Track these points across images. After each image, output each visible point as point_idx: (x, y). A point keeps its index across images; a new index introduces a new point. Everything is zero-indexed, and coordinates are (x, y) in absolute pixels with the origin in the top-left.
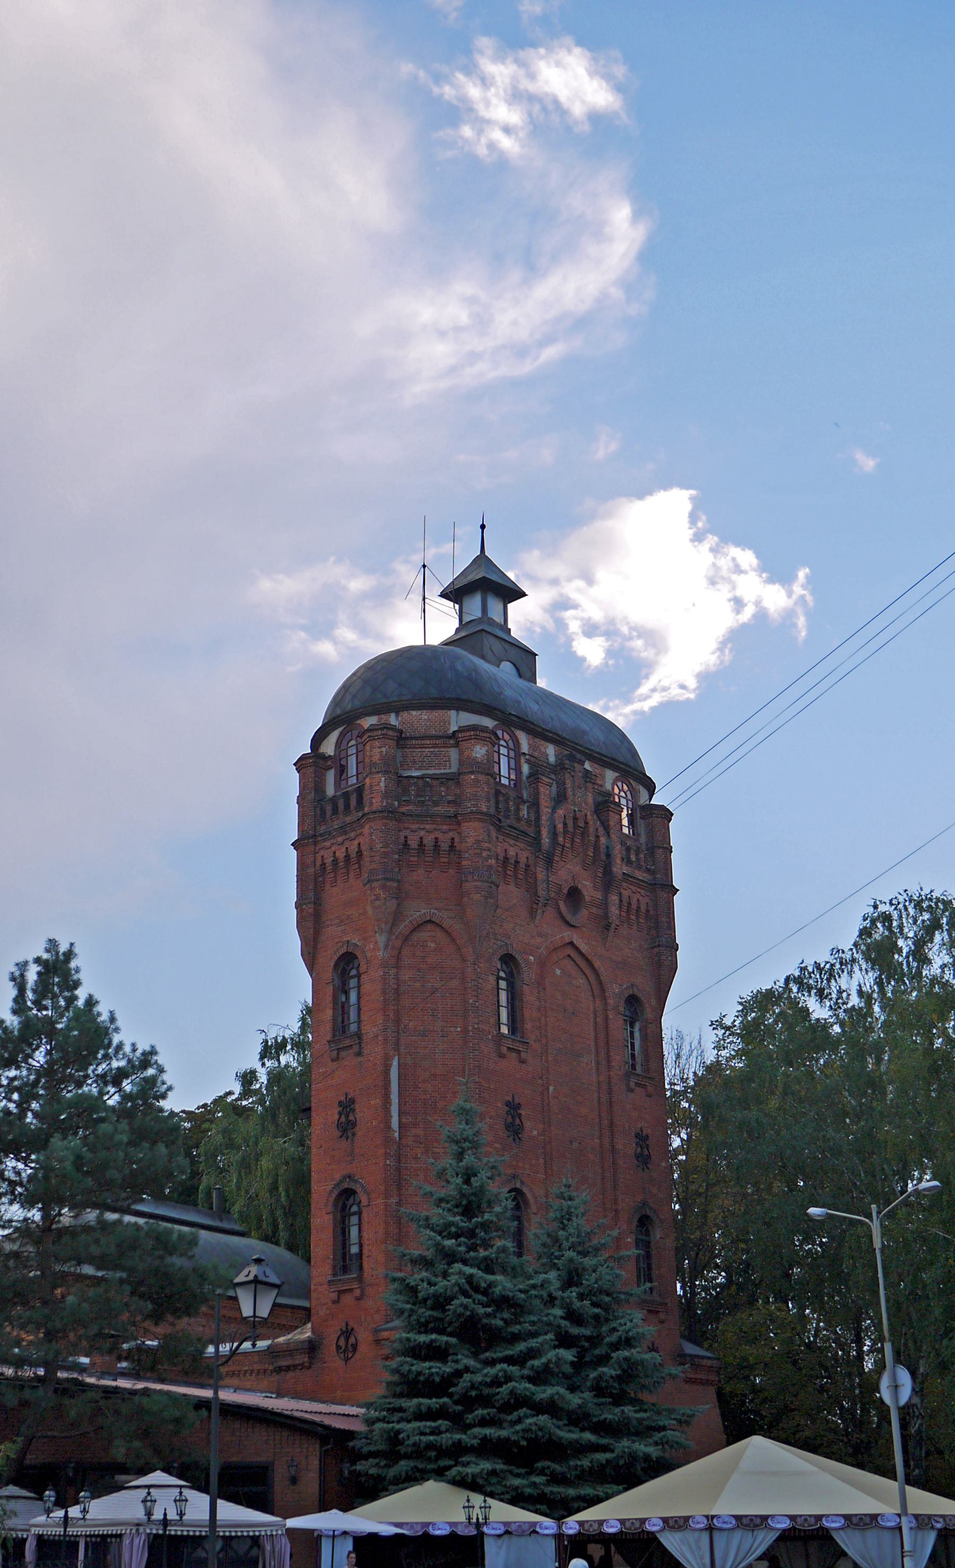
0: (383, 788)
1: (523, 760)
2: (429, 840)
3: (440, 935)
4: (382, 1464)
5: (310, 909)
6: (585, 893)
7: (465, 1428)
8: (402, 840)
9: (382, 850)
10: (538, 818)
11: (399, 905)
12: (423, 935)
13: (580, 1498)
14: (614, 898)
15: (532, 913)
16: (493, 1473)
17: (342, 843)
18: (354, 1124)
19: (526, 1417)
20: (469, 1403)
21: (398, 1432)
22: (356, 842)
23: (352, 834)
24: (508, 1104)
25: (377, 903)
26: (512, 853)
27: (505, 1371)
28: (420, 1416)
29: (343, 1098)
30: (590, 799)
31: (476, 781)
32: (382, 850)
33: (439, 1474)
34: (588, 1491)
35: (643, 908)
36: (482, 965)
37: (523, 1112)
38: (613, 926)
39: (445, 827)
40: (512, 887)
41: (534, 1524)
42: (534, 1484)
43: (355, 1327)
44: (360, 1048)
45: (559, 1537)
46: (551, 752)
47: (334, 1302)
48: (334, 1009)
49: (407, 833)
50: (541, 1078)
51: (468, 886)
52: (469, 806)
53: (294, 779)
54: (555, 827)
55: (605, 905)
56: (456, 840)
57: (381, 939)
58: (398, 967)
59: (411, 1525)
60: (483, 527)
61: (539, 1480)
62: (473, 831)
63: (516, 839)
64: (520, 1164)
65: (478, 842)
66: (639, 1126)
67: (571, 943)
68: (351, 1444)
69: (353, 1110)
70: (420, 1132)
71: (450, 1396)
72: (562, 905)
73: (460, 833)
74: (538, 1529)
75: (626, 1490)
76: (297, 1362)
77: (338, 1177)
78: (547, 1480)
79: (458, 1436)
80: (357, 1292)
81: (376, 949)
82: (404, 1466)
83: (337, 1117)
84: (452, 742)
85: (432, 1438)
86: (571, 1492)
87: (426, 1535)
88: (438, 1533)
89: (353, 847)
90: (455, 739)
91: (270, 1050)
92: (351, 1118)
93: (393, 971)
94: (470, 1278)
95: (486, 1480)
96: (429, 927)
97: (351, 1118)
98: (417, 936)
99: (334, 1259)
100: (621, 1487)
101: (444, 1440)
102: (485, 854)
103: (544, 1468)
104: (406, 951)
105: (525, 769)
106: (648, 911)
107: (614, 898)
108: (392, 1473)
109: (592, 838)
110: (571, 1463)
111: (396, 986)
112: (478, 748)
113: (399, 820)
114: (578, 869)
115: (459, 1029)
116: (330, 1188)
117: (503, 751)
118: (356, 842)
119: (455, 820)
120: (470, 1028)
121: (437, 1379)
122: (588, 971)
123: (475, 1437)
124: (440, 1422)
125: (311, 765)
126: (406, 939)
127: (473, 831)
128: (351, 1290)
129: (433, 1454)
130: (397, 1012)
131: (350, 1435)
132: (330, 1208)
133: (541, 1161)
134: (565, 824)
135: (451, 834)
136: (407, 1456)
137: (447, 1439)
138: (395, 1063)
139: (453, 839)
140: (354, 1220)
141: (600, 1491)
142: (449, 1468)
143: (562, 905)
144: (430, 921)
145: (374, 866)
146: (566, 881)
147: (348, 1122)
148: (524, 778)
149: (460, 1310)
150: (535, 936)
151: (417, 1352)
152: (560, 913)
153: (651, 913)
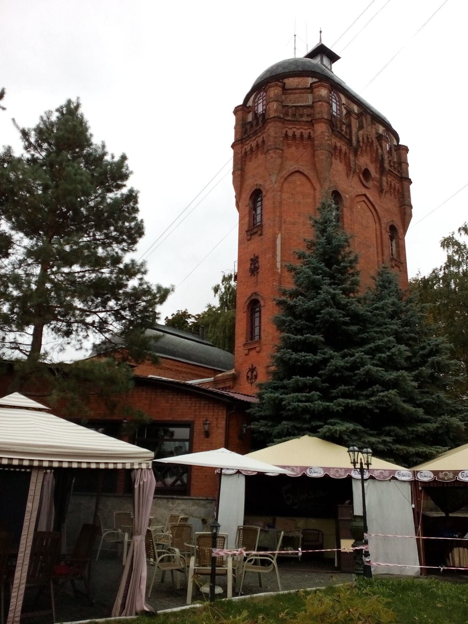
1: (343, 107)
2: (298, 133)
3: (303, 179)
4: (269, 424)
5: (239, 173)
7: (331, 400)
8: (284, 132)
13: (418, 454)
16: (354, 432)
17: (255, 139)
18: (257, 268)
19: (378, 391)
20: (333, 380)
21: (282, 400)
22: (261, 137)
23: (260, 134)
25: (272, 160)
26: (338, 144)
27: (362, 358)
28: (298, 389)
29: (253, 257)
31: (321, 105)
33: (313, 431)
34: (422, 449)
35: (397, 188)
38: (384, 191)
39: (306, 127)
40: (338, 161)
41: (394, 472)
42: (384, 442)
43: (256, 366)
44: (262, 232)
45: (414, 483)
47: (247, 355)
48: (249, 217)
49: (287, 129)
51: (318, 153)
52: (318, 116)
53: (232, 120)
54: (358, 138)
55: (380, 182)
56: (312, 133)
57: (274, 178)
59: (292, 468)
60: (321, 32)
61: (388, 439)
63: (340, 139)
65: (323, 132)
67: (365, 195)
68: (248, 411)
69: (258, 262)
71: (320, 376)
73: (313, 130)
74: (396, 476)
75: (449, 449)
76: (227, 385)
77: (249, 294)
78: (393, 440)
79: (328, 404)
80: (258, 349)
81: (270, 184)
82: (285, 424)
83: (249, 266)
85: (307, 404)
86: (412, 450)
87: (304, 476)
88: (314, 475)
89: (260, 140)
91: (226, 279)
93: (279, 193)
94: (334, 296)
95: (349, 436)
96: (297, 174)
97: (257, 265)
98: (290, 179)
99: (247, 334)
100: (447, 448)
101: (316, 406)
103: (390, 431)
104: (286, 185)
108: (277, 430)
109: (375, 148)
110: (410, 429)
112: (323, 90)
113: (283, 123)
114: (368, 162)
116: (246, 300)
117: (333, 100)
118: (261, 137)
119: (311, 123)
121: (311, 364)
122: (373, 210)
123: (339, 405)
124: (313, 392)
125: (241, 111)
127: (321, 128)
128: (255, 348)
129: (308, 416)
131: (248, 405)
132: (245, 310)
134: (363, 139)
135: (309, 131)
136: (288, 418)
137: (320, 404)
138: (279, 236)
139: (310, 133)
140: (257, 315)
141: (432, 450)
142: (321, 427)
143: (361, 176)
147: (255, 267)
149: (327, 317)
150: (350, 187)
151: (296, 347)
153: (400, 191)
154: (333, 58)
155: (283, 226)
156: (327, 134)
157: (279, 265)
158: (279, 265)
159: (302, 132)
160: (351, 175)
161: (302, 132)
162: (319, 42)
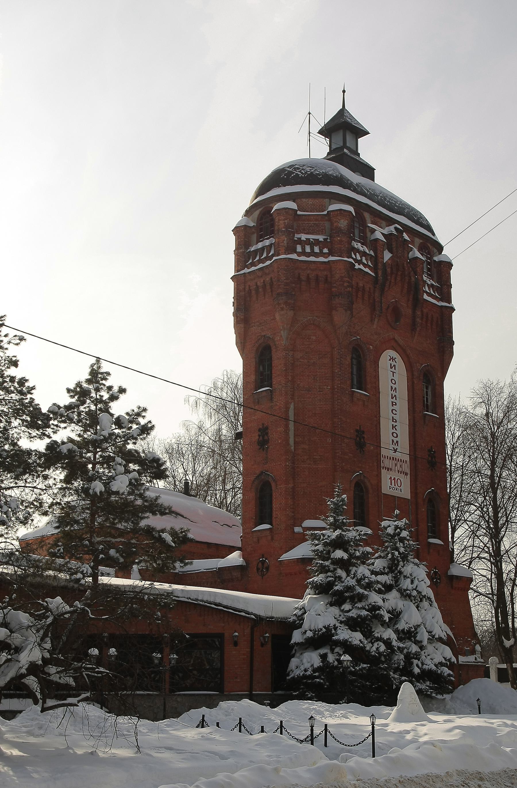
0: (286, 245)
9: (285, 281)
11: (294, 314)
14: (419, 313)
15: (372, 320)
24: (357, 431)
25: (282, 312)
26: (361, 285)
31: (341, 241)
32: (285, 281)
36: (343, 350)
37: (365, 436)
38: (418, 329)
50: (376, 417)
54: (386, 270)
57: (284, 334)
60: (344, 91)
67: (394, 339)
69: (267, 434)
77: (258, 472)
81: (282, 339)
83: (257, 438)
84: (326, 218)
92: (266, 438)
93: (291, 353)
97: (266, 438)
111: (292, 362)
112: (342, 221)
115: (329, 387)
133: (375, 464)
134: (392, 268)
138: (292, 406)
139: (327, 276)
145: (280, 290)
153: (439, 323)
154: (360, 132)
156: (347, 279)
157: (292, 441)
158: (292, 441)
159: (317, 275)
161: (317, 275)
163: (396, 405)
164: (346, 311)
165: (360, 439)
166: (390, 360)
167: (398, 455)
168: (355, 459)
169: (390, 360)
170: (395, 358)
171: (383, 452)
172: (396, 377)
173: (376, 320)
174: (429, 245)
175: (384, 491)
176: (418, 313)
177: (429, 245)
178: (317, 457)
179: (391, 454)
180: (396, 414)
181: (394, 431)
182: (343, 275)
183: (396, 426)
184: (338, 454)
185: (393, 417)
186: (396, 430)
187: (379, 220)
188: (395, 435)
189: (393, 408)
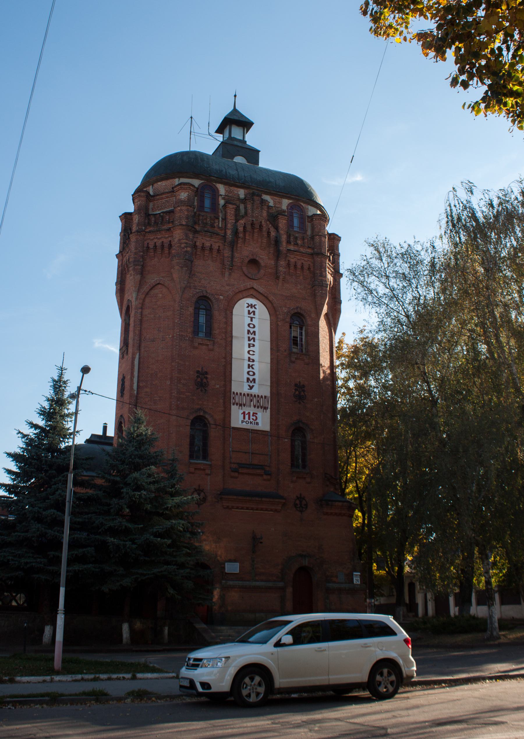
6: (261, 261)
8: (146, 245)
10: (226, 226)
12: (155, 291)
15: (223, 274)
26: (208, 244)
30: (265, 214)
35: (306, 267)
36: (184, 302)
37: (209, 376)
38: (281, 277)
46: (242, 193)
49: (149, 241)
50: (225, 358)
54: (237, 229)
58: (142, 308)
60: (235, 96)
62: (178, 234)
63: (211, 237)
64: (205, 403)
65: (179, 240)
66: (298, 380)
67: (253, 288)
70: (148, 390)
72: (245, 269)
90: (173, 191)
93: (140, 310)
96: (160, 286)
102: (183, 246)
104: (147, 300)
105: (222, 202)
106: (309, 269)
107: (282, 263)
112: (182, 194)
120: (175, 335)
126: (147, 294)
130: (140, 331)
133: (221, 401)
134: (245, 227)
135: (170, 239)
139: (170, 241)
143: (245, 269)
144: (159, 284)
146: (247, 257)
148: (221, 207)
152: (244, 273)
155: (143, 345)
156: (184, 241)
160: (227, 274)
162: (232, 108)
163: (254, 346)
164: (182, 267)
165: (202, 380)
166: (248, 307)
167: (255, 391)
168: (195, 398)
169: (248, 307)
170: (255, 305)
171: (235, 388)
172: (255, 322)
173: (227, 274)
174: (302, 204)
175: (233, 425)
176: (281, 263)
177: (302, 204)
178: (157, 398)
179: (246, 389)
180: (253, 355)
181: (251, 369)
182: (181, 238)
183: (252, 365)
184: (173, 394)
185: (249, 358)
186: (253, 368)
187: (236, 189)
188: (251, 373)
189: (249, 349)
